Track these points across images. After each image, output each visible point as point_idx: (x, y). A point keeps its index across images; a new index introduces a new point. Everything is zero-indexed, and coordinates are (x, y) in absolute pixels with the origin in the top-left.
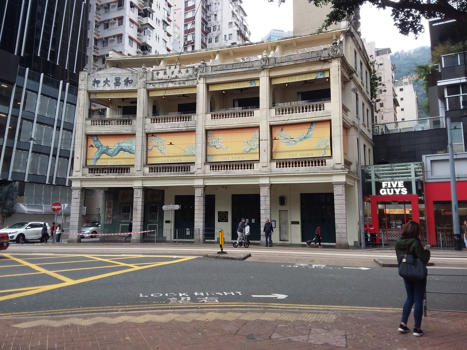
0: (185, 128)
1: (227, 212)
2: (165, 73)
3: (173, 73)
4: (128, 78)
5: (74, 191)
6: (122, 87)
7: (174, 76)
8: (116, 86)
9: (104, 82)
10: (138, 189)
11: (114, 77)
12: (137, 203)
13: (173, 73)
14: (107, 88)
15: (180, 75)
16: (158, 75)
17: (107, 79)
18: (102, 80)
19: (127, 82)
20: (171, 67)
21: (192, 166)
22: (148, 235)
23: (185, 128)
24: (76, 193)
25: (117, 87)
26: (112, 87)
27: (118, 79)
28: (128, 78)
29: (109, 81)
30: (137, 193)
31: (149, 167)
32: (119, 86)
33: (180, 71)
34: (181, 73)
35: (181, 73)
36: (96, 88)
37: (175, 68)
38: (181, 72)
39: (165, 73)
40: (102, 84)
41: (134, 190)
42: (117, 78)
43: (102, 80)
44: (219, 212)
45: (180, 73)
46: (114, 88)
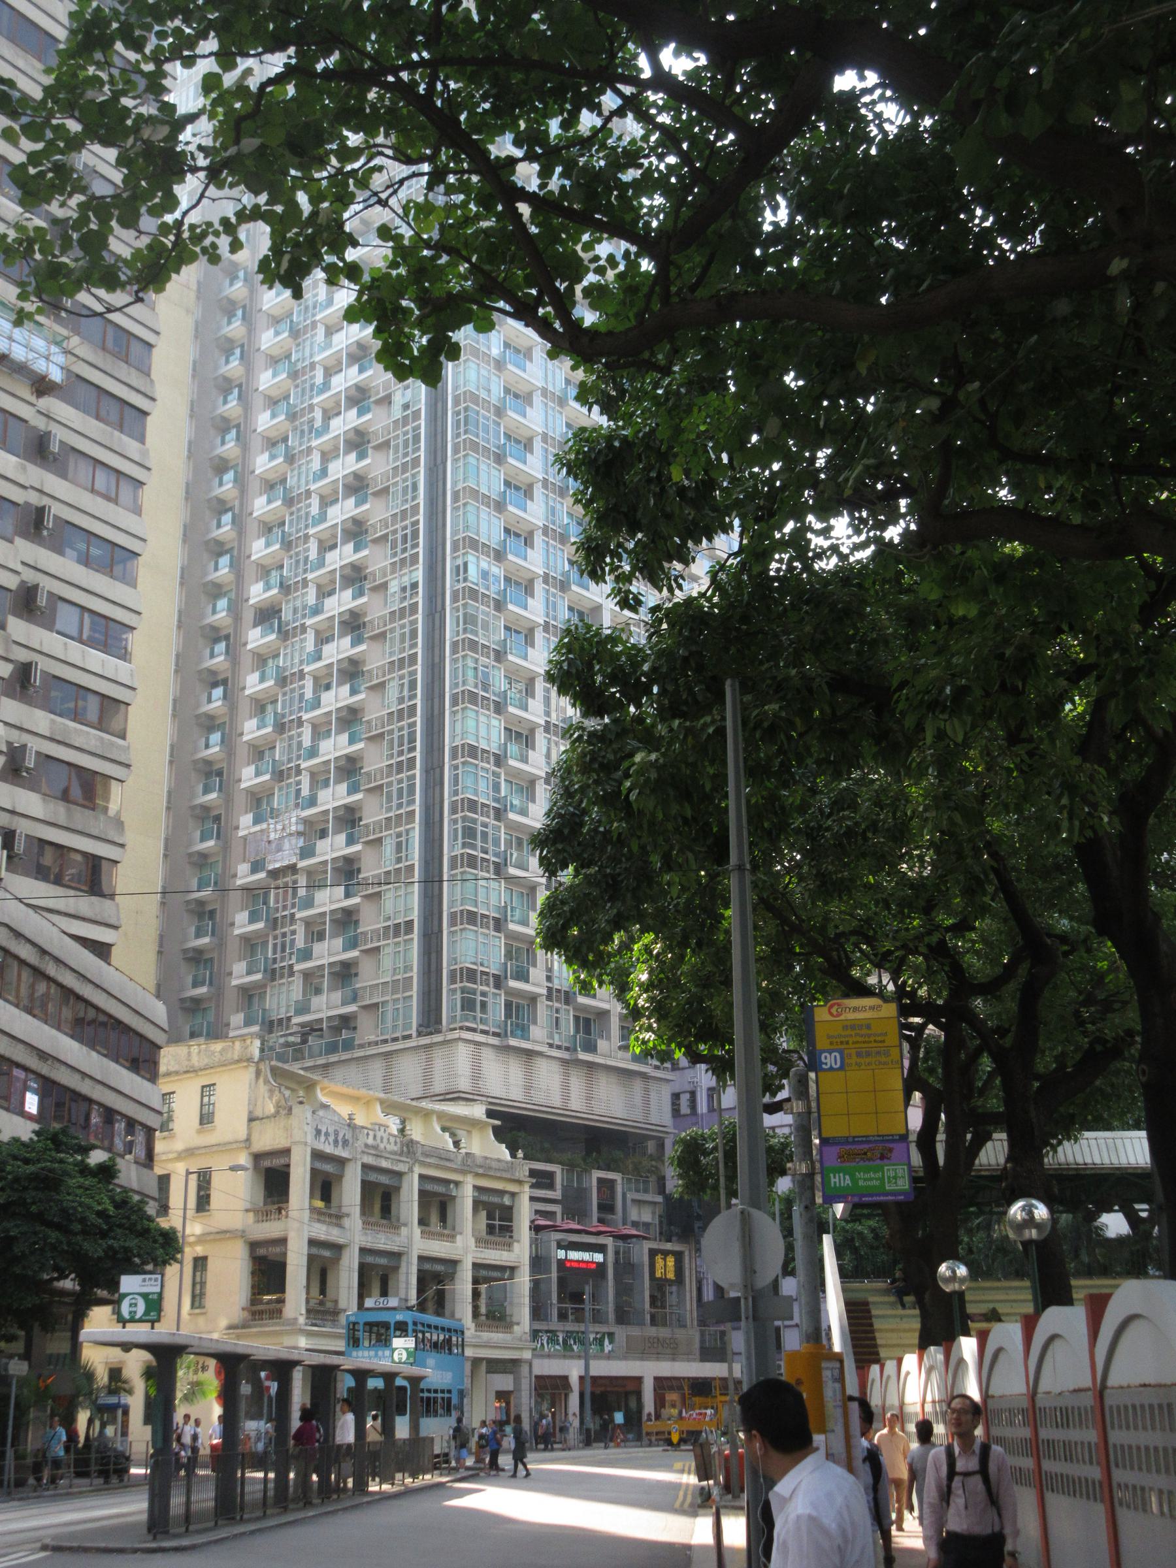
43: (324, 1130)
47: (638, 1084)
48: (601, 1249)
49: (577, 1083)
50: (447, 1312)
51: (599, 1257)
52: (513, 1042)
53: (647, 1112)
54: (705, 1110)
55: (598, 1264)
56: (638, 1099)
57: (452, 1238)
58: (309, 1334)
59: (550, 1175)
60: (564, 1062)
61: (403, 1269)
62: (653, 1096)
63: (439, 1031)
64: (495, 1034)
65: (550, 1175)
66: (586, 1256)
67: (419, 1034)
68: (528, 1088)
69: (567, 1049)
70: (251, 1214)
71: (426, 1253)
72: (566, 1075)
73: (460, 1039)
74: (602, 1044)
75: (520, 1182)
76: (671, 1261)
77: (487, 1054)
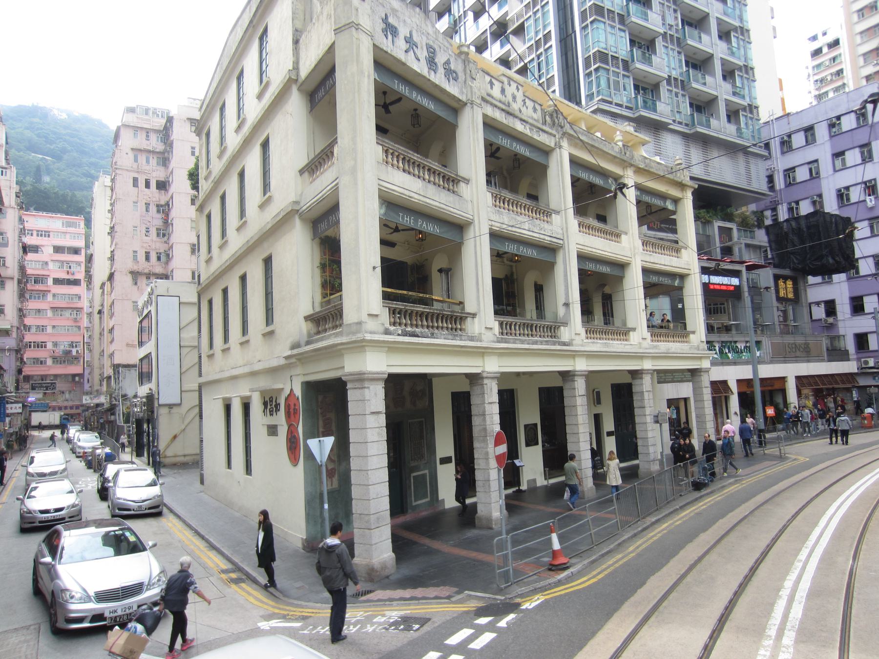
0: (549, 239)
1: (536, 425)
4: (448, 62)
5: (372, 387)
6: (438, 78)
10: (490, 380)
13: (514, 98)
15: (524, 109)
16: (492, 88)
20: (512, 83)
21: (562, 328)
23: (549, 239)
24: (376, 394)
26: (420, 67)
30: (491, 389)
31: (499, 321)
34: (527, 108)
35: (527, 108)
37: (518, 89)
39: (503, 91)
41: (486, 381)
43: (403, 32)
44: (526, 426)
47: (741, 158)
48: (736, 274)
49: (696, 155)
50: (617, 321)
51: (735, 281)
53: (749, 179)
54: (783, 186)
55: (735, 286)
56: (742, 170)
57: (616, 235)
58: (392, 348)
60: (685, 136)
61: (559, 269)
62: (753, 167)
64: (627, 107)
66: (725, 280)
69: (687, 125)
70: (306, 174)
71: (587, 250)
72: (687, 146)
74: (714, 122)
75: (682, 186)
76: (790, 284)
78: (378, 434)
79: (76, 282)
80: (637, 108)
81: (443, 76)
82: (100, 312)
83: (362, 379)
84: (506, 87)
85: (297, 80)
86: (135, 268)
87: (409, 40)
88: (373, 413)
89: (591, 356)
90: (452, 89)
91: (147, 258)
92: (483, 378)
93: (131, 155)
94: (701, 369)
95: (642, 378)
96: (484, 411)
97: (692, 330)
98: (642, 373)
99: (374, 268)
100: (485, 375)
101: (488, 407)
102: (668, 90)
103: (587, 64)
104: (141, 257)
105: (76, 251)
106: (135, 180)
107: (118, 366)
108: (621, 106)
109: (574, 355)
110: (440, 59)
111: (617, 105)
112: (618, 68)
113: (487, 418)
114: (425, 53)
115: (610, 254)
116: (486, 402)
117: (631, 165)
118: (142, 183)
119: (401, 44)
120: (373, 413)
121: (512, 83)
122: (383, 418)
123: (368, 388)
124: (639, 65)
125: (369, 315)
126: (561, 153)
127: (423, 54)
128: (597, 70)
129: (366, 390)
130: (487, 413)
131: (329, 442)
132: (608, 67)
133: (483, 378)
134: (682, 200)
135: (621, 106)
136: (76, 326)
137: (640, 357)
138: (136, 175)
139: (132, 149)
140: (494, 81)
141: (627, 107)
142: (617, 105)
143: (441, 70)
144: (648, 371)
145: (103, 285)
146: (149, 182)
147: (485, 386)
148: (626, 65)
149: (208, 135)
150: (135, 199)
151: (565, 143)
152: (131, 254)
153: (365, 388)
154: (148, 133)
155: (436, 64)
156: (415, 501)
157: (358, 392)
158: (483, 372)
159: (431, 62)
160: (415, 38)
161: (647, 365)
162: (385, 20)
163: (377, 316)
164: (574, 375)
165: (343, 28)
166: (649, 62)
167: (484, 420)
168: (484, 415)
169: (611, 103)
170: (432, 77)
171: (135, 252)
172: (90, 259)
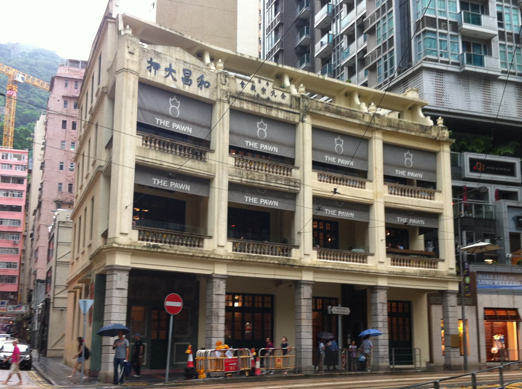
2: (253, 88)
3: (264, 90)
4: (202, 77)
7: (264, 96)
8: (184, 84)
9: (166, 70)
10: (219, 280)
11: (182, 66)
12: (218, 304)
13: (264, 90)
14: (170, 83)
17: (170, 65)
18: (164, 65)
19: (201, 83)
20: (262, 81)
22: (175, 363)
24: (121, 278)
25: (187, 86)
27: (187, 73)
28: (202, 77)
29: (174, 72)
30: (219, 286)
31: (233, 242)
32: (189, 85)
33: (273, 93)
34: (276, 96)
35: (276, 96)
36: (150, 76)
37: (267, 84)
38: (275, 94)
39: (253, 88)
40: (162, 72)
42: (187, 70)
43: (164, 65)
45: (273, 96)
46: (182, 88)
52: (469, 68)
58: (134, 252)
59: (512, 165)
63: (410, 66)
65: (512, 165)
67: (399, 73)
68: (487, 103)
73: (422, 69)
77: (448, 80)
78: (121, 301)
79: (17, 209)
80: (463, 64)
81: (196, 87)
82: (32, 235)
83: (113, 269)
84: (257, 84)
85: (107, 93)
86: (60, 198)
87: (170, 71)
88: (117, 289)
89: (315, 269)
90: (204, 93)
91: (70, 189)
92: (213, 278)
93: (62, 102)
94: (447, 291)
95: (376, 293)
96: (212, 300)
97: (443, 259)
98: (377, 289)
99: (126, 207)
100: (214, 276)
101: (215, 297)
102: (500, 44)
103: (417, 29)
104: (65, 188)
105: (19, 180)
106: (64, 122)
107: (38, 281)
108: (448, 63)
109: (302, 268)
110: (194, 77)
111: (442, 62)
112: (446, 29)
113: (214, 303)
114: (182, 75)
115: (349, 197)
116: (214, 293)
117: (378, 129)
118: (69, 125)
119: (162, 72)
120: (117, 289)
121: (262, 81)
122: (125, 293)
123: (116, 274)
124: (466, 26)
125: (121, 234)
126: (303, 126)
127: (179, 76)
128: (425, 32)
129: (115, 276)
130: (214, 301)
131: (90, 302)
132: (434, 30)
133: (213, 278)
134: (440, 153)
135: (448, 63)
136: (14, 249)
137: (377, 275)
138: (65, 119)
139: (63, 97)
140: (245, 82)
141: (453, 64)
142: (442, 62)
143: (195, 83)
144: (382, 288)
145: (35, 211)
146: (75, 124)
147: (214, 283)
148: (455, 26)
149: (82, 109)
150: (63, 139)
151: (307, 119)
152: (57, 186)
153: (114, 274)
154: (76, 82)
155: (191, 80)
156: (176, 361)
157: (111, 276)
158: (213, 274)
159: (187, 80)
160: (173, 67)
161: (382, 283)
162: (150, 62)
163: (127, 234)
164: (301, 284)
165: (120, 71)
166: (478, 22)
167: (212, 305)
168: (212, 302)
169: (437, 61)
170: (187, 89)
171: (60, 184)
172: (29, 187)
